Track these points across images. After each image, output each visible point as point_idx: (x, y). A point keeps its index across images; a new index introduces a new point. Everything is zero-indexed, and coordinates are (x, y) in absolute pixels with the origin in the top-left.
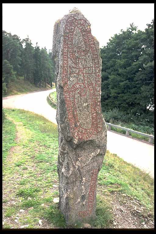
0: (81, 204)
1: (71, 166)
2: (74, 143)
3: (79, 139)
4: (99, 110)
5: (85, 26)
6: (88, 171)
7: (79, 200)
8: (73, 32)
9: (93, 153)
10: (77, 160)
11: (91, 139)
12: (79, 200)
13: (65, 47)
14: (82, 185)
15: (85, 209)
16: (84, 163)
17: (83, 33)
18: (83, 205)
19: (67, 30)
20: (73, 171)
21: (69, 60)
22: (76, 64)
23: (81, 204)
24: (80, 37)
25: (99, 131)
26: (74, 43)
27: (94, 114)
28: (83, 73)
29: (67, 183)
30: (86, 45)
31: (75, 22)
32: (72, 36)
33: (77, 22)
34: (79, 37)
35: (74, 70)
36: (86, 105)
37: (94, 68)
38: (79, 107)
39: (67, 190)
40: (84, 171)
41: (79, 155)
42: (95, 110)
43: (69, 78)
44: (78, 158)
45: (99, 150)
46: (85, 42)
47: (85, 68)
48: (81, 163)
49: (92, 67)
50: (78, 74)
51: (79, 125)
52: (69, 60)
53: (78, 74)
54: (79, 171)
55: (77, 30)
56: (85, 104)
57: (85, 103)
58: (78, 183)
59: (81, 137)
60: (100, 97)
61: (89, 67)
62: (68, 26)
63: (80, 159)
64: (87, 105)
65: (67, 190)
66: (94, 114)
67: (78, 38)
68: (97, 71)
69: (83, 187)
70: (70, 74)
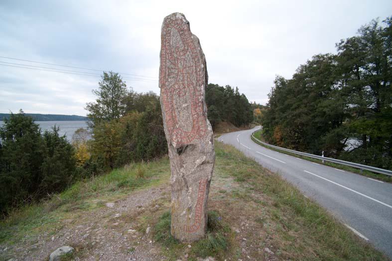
6: (195, 180)
8: (170, 33)
9: (198, 160)
10: (182, 166)
11: (192, 143)
12: (184, 212)
14: (187, 196)
18: (190, 219)
21: (167, 61)
22: (174, 65)
23: (187, 216)
27: (196, 116)
28: (183, 73)
35: (173, 71)
37: (194, 68)
38: (177, 108)
40: (190, 180)
42: (196, 111)
43: (168, 79)
45: (205, 157)
46: (183, 42)
49: (192, 66)
52: (167, 61)
54: (185, 179)
55: (174, 31)
58: (184, 192)
59: (180, 140)
61: (189, 67)
63: (184, 166)
64: (187, 106)
67: (175, 40)
69: (189, 198)
70: (169, 75)
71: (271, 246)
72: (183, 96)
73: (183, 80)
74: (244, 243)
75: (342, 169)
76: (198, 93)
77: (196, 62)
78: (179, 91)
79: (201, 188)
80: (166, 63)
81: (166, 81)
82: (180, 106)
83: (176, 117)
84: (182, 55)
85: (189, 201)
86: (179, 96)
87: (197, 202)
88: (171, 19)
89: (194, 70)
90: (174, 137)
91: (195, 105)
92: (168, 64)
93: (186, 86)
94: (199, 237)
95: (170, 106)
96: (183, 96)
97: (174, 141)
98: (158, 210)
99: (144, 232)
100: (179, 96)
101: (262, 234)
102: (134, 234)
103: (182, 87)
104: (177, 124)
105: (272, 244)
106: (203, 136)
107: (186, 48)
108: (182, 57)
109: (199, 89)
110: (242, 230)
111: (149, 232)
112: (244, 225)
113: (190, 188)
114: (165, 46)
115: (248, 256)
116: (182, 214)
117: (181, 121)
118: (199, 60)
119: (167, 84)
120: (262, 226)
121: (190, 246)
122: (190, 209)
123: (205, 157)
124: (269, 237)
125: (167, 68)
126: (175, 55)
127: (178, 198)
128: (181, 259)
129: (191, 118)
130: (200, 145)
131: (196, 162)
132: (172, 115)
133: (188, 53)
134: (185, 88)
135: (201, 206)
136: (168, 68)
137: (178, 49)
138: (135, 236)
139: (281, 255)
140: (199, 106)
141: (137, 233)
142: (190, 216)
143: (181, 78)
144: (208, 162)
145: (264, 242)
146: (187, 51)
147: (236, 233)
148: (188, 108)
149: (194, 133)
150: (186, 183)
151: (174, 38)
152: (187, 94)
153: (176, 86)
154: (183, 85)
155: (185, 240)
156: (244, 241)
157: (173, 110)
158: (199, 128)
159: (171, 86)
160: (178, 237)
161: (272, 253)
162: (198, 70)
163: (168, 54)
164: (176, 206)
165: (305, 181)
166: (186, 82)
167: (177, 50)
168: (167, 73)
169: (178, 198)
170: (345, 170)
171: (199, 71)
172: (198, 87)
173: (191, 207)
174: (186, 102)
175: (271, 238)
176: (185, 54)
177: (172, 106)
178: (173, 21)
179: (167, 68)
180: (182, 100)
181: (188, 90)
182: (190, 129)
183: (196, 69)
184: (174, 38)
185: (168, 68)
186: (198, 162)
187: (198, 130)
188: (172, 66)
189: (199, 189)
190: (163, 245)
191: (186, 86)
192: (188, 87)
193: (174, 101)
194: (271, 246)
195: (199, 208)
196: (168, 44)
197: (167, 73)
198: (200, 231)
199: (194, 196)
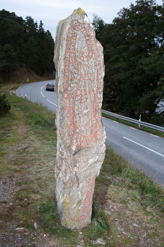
0: (77, 209)
1: (68, 171)
2: (73, 150)
3: (77, 146)
4: (99, 117)
5: (89, 30)
6: (86, 177)
7: (75, 205)
8: (76, 37)
10: (75, 166)
13: (67, 52)
14: (78, 191)
15: (81, 214)
16: (82, 170)
17: (87, 38)
18: (79, 210)
19: (71, 34)
20: (70, 177)
21: (71, 65)
23: (77, 209)
24: (83, 42)
25: (99, 138)
26: (76, 47)
27: (95, 122)
28: (85, 79)
29: (64, 188)
30: (89, 51)
31: (79, 25)
32: (75, 41)
33: (81, 25)
34: (82, 41)
36: (87, 112)
37: (96, 75)
38: (79, 114)
39: (63, 195)
40: (81, 177)
41: (77, 161)
42: (95, 117)
43: (70, 84)
44: (76, 164)
46: (88, 48)
47: (87, 74)
48: (79, 169)
49: (94, 73)
50: (79, 80)
51: (78, 132)
53: (79, 80)
54: (77, 177)
56: (85, 111)
57: (86, 110)
58: (75, 188)
59: (79, 144)
60: (102, 104)
62: (72, 30)
63: (77, 165)
64: (88, 112)
65: (63, 195)
66: (95, 122)
68: (100, 77)
69: (79, 192)
70: (71, 80)
71: (138, 222)
72: (84, 102)
73: (85, 86)
74: (117, 223)
75: (156, 134)
76: (97, 101)
77: (98, 69)
78: (81, 98)
79: (90, 183)
80: (69, 68)
81: (69, 86)
82: (82, 111)
83: (76, 122)
84: (85, 60)
85: (79, 195)
86: (81, 102)
87: (87, 195)
88: (78, 22)
89: (96, 77)
90: (75, 141)
91: (96, 111)
92: (71, 68)
93: (88, 93)
94: (87, 224)
95: (72, 111)
96: (84, 102)
97: (73, 145)
98: (29, 204)
99: (33, 228)
100: (81, 102)
101: (128, 213)
102: (25, 232)
103: (83, 93)
104: (78, 128)
105: (138, 220)
106: (98, 139)
107: (91, 55)
108: (85, 63)
109: (99, 97)
110: (112, 212)
111: (37, 227)
112: (112, 208)
113: (81, 184)
114: (70, 49)
115: (124, 233)
116: (73, 208)
117: (81, 126)
118: (101, 68)
119: (69, 89)
120: (127, 207)
121: (81, 233)
122: (79, 202)
123: (97, 157)
124: (134, 215)
125: (70, 73)
126: (79, 60)
127: (69, 194)
128: (79, 244)
129: (90, 123)
130: (95, 147)
131: (89, 162)
132: (73, 120)
133: (92, 60)
134: (86, 94)
135: (89, 198)
136: (71, 72)
137: (82, 54)
138: (27, 233)
139: (146, 227)
140: (98, 113)
141: (27, 230)
142: (80, 208)
143: (83, 84)
144: (100, 161)
145: (132, 219)
146: (91, 58)
147: (109, 215)
148: (88, 114)
149: (92, 137)
150: (78, 180)
151: (80, 42)
152: (88, 100)
153: (79, 92)
154: (85, 91)
155: (75, 229)
156: (116, 221)
157: (74, 115)
158: (96, 132)
159: (74, 92)
160: (69, 227)
161: (139, 227)
162: (100, 77)
163: (72, 57)
164: (68, 201)
165: (125, 148)
166: (88, 89)
167: (81, 55)
168: (70, 78)
169: (69, 194)
170: (159, 135)
171: (100, 79)
172: (98, 95)
173: (81, 200)
174: (87, 109)
175: (136, 216)
176: (88, 60)
177: (74, 112)
178: (80, 24)
179: (70, 73)
180: (84, 106)
181: (89, 97)
182: (89, 133)
183: (97, 76)
184: (80, 42)
185: (71, 72)
186: (91, 161)
187: (95, 134)
188: (75, 70)
189: (89, 184)
190: (58, 236)
191: (88, 93)
192: (89, 93)
193: (76, 108)
194: (138, 222)
195: (88, 200)
196: (73, 47)
197: (70, 78)
198: (88, 220)
199: (83, 190)
